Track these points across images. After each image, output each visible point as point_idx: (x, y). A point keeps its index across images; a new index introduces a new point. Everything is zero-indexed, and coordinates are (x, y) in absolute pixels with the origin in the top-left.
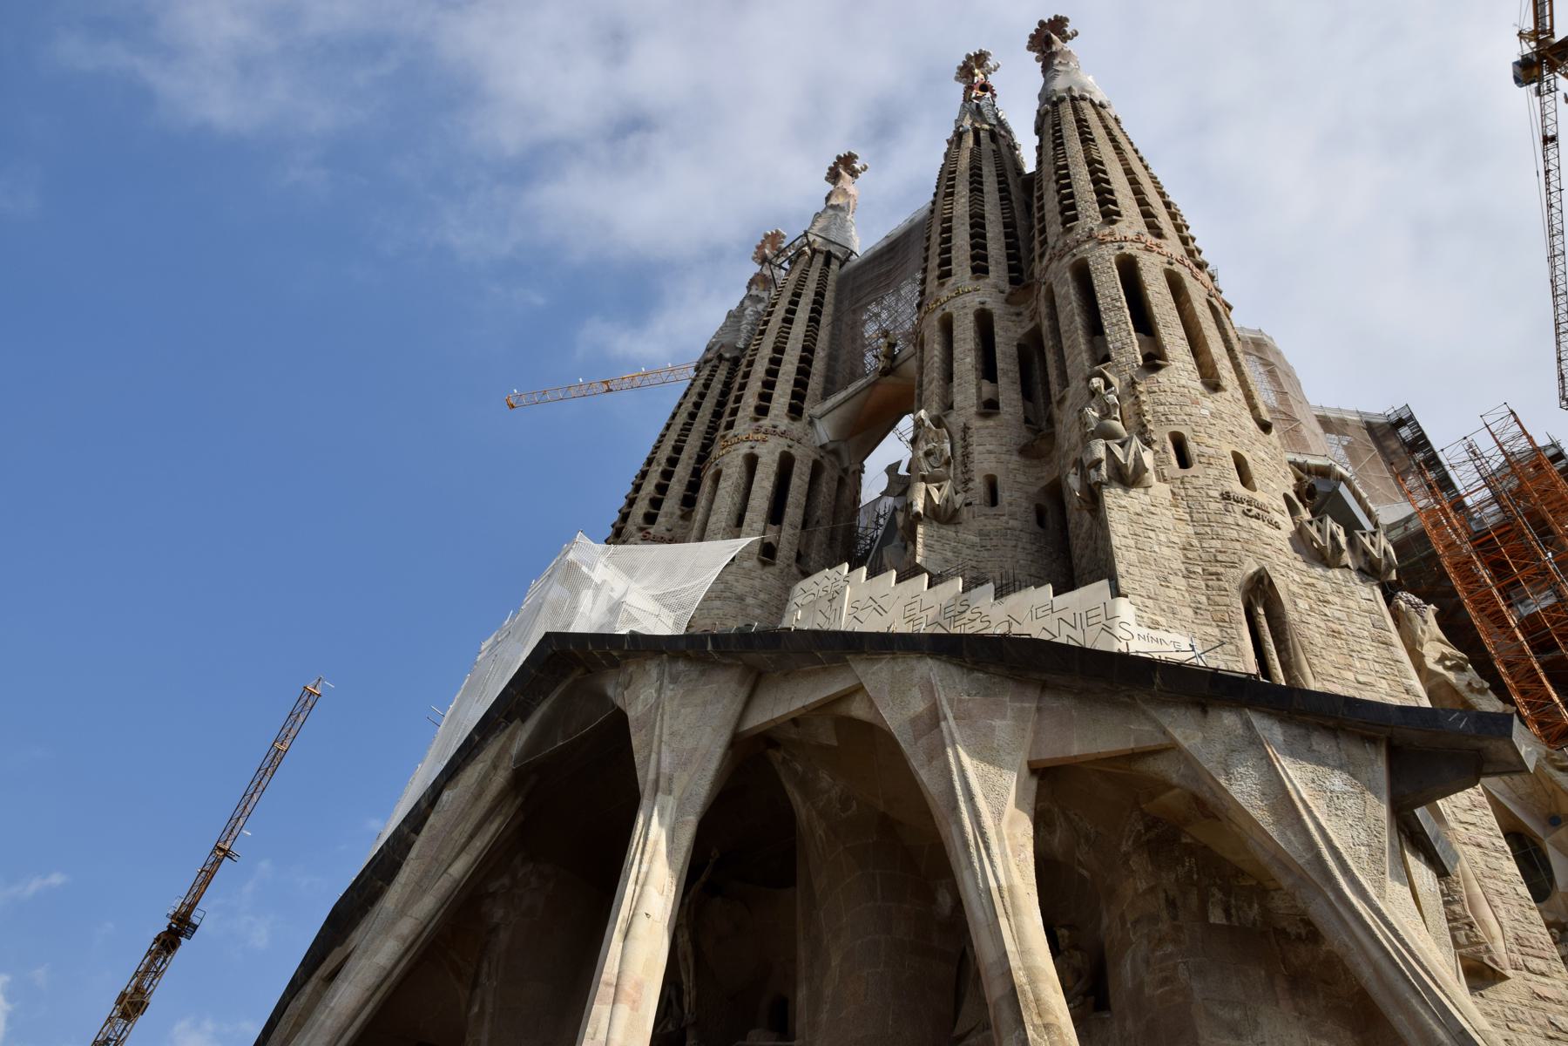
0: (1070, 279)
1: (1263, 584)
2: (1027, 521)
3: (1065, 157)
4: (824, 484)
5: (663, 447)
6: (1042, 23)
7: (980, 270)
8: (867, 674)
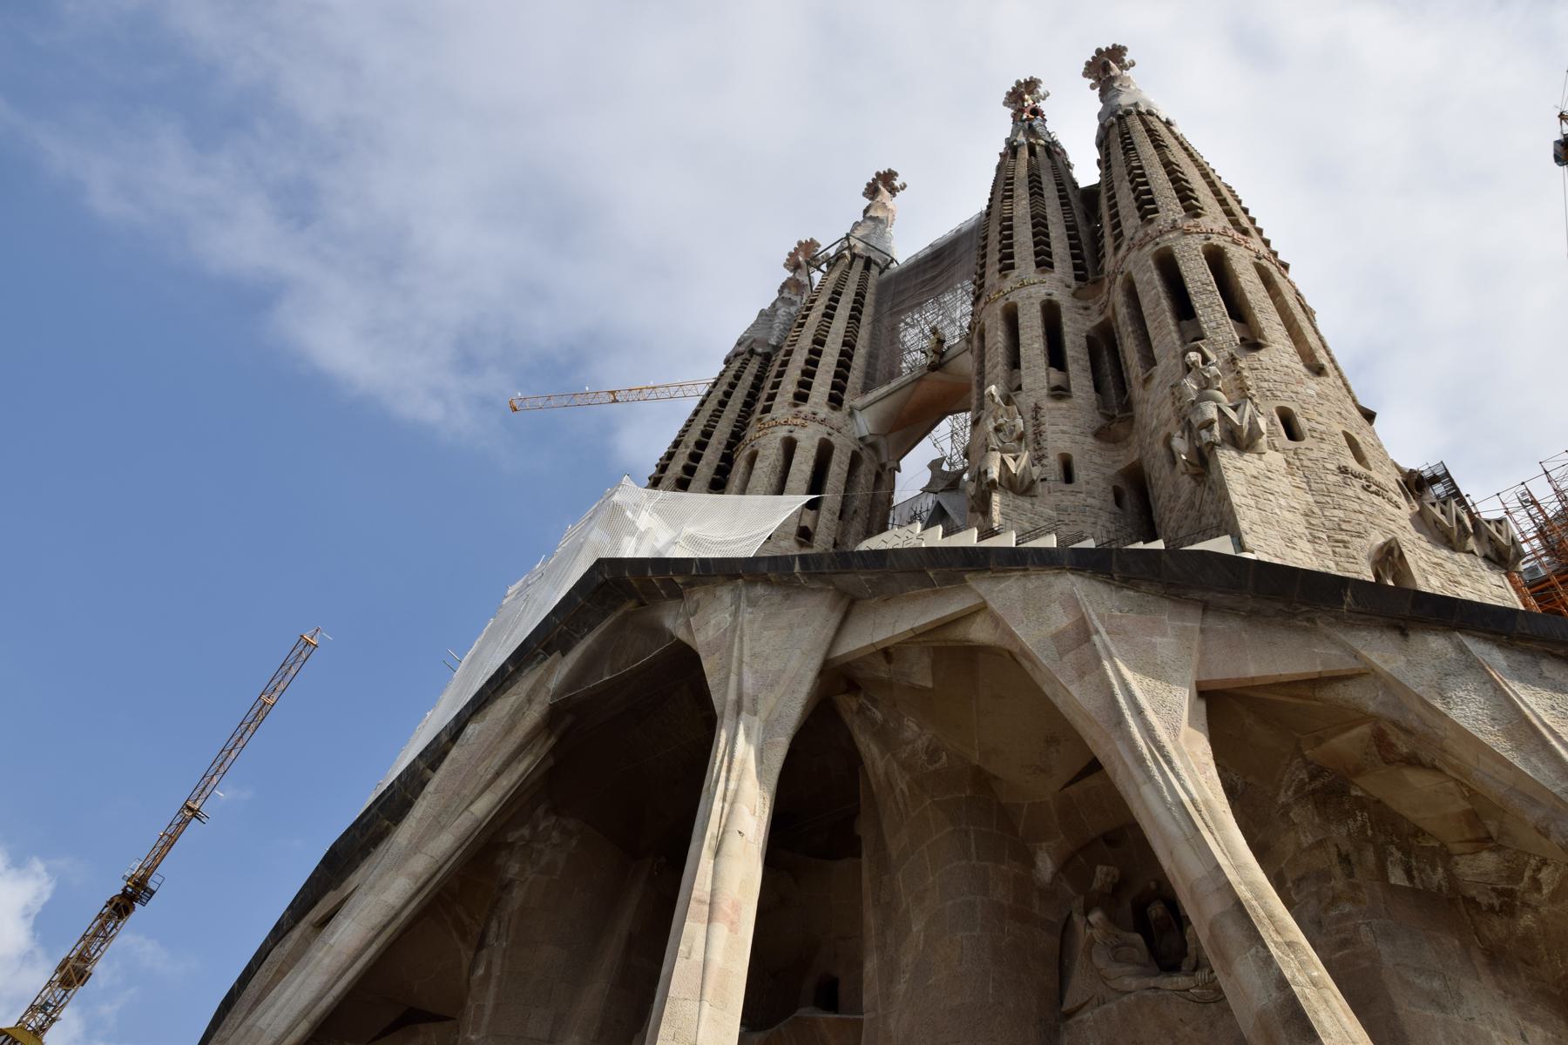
0: (1153, 266)
1: (1393, 557)
2: (1105, 500)
3: (1138, 159)
4: (862, 476)
5: (691, 430)
6: (1099, 51)
8: (993, 591)
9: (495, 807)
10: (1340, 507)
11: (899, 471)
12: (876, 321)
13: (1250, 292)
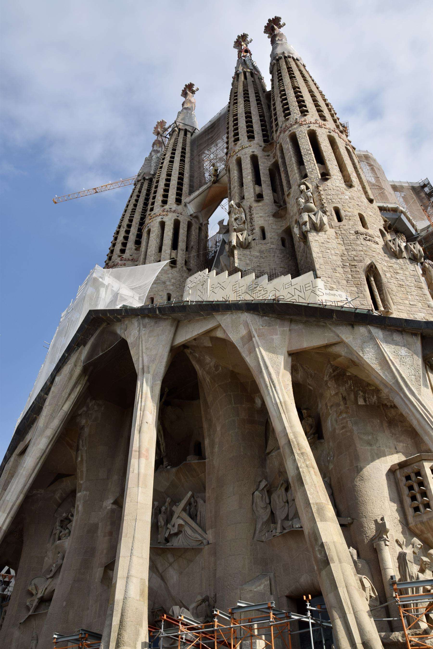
0: (289, 141)
2: (278, 245)
3: (283, 85)
5: (124, 220)
7: (251, 137)
10: (355, 250)
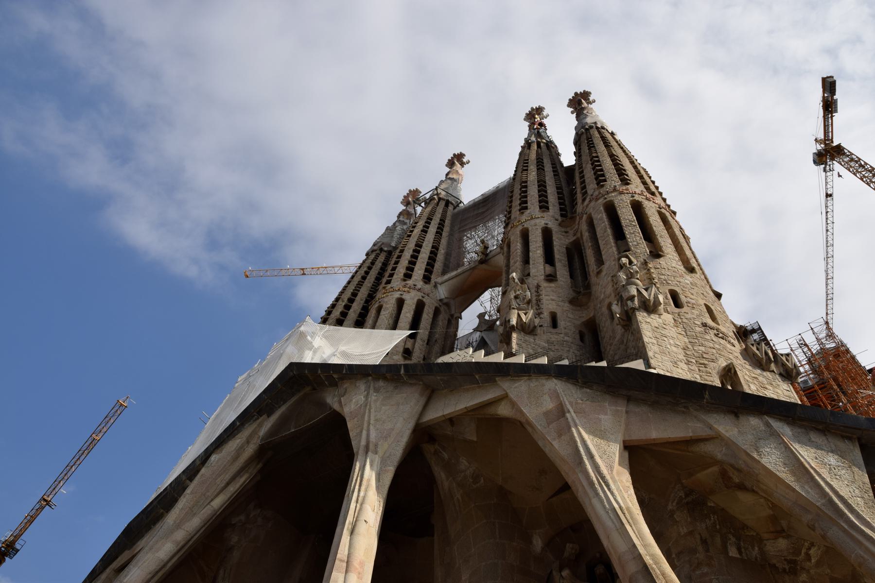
0: (603, 210)
1: (731, 373)
3: (596, 152)
4: (441, 321)
5: (346, 292)
6: (576, 94)
8: (511, 388)
9: (225, 503)
10: (702, 345)
11: (461, 319)
12: (451, 235)
13: (655, 226)
